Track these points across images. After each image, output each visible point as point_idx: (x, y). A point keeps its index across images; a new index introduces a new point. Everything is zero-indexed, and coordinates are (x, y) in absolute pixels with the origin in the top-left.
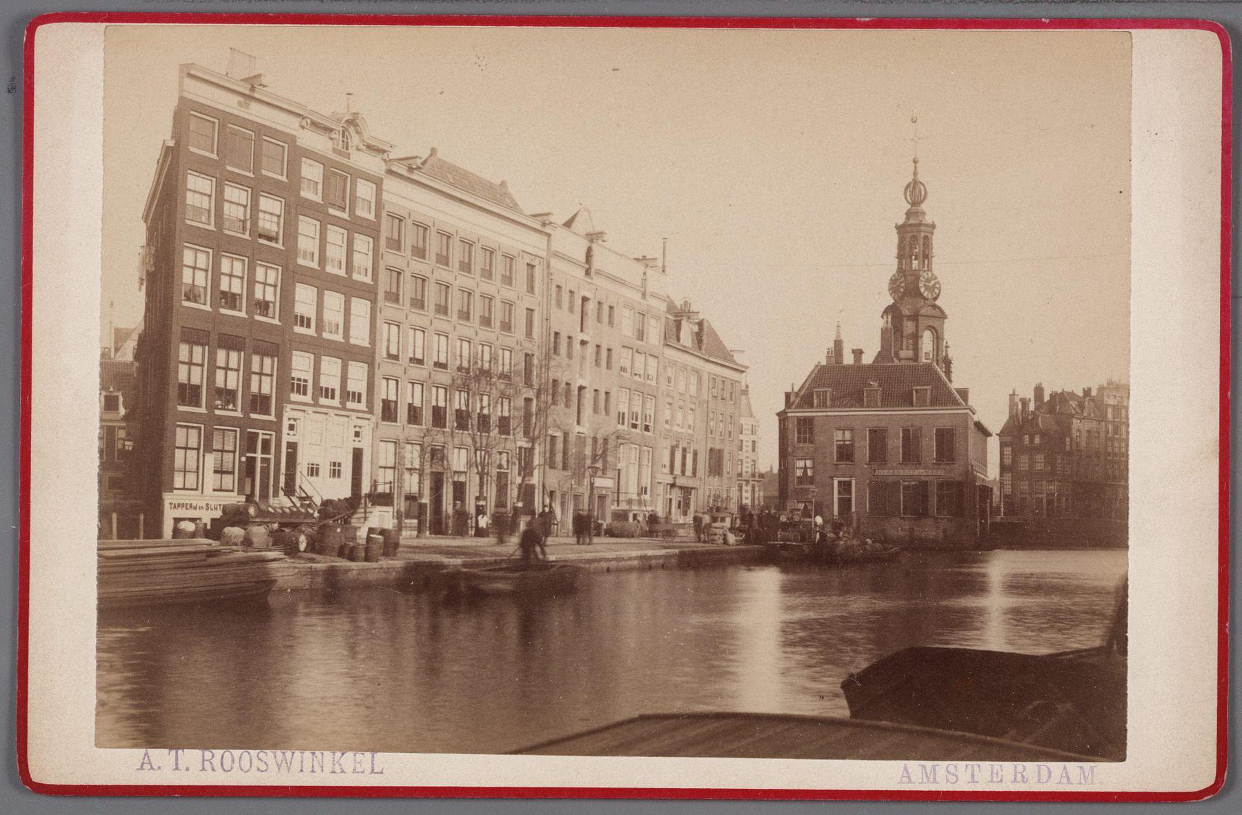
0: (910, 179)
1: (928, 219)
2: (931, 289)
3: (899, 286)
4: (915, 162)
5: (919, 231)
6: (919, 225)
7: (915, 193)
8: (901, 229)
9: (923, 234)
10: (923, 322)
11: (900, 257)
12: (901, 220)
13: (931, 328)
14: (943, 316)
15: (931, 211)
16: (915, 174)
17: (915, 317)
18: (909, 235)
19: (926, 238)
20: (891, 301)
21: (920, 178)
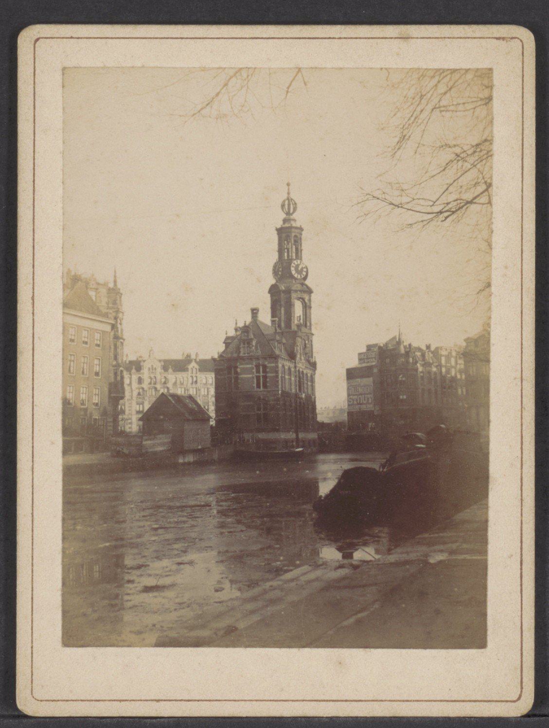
0: (285, 196)
1: (298, 224)
2: (299, 272)
3: (278, 271)
4: (288, 185)
5: (291, 232)
6: (291, 227)
7: (289, 207)
8: (280, 231)
9: (293, 234)
10: (294, 295)
11: (281, 251)
12: (279, 224)
13: (299, 299)
14: (310, 291)
15: (300, 218)
16: (289, 193)
17: (288, 292)
18: (284, 235)
19: (296, 236)
20: (273, 282)
21: (292, 196)
